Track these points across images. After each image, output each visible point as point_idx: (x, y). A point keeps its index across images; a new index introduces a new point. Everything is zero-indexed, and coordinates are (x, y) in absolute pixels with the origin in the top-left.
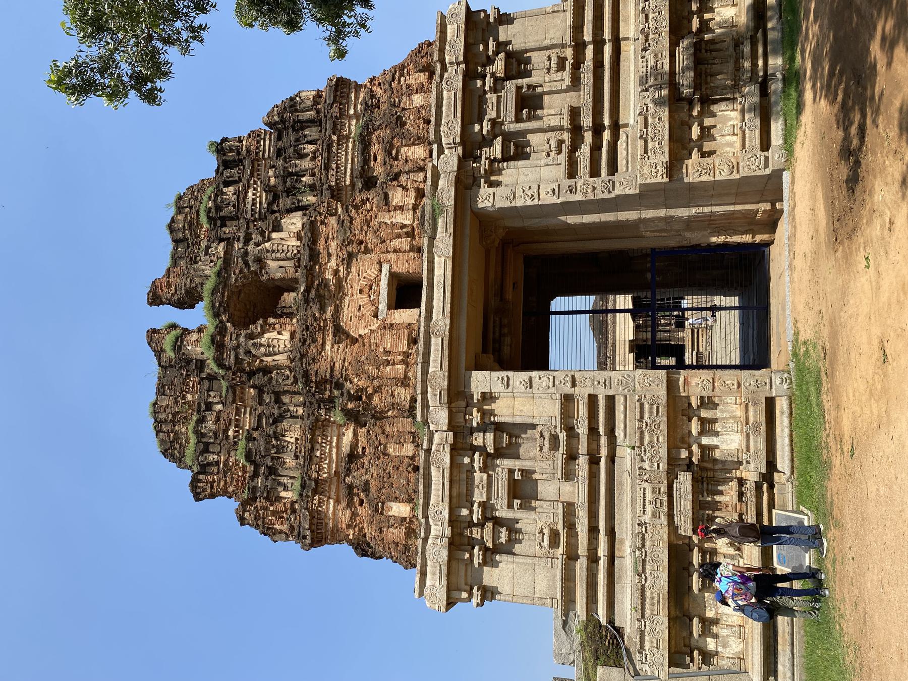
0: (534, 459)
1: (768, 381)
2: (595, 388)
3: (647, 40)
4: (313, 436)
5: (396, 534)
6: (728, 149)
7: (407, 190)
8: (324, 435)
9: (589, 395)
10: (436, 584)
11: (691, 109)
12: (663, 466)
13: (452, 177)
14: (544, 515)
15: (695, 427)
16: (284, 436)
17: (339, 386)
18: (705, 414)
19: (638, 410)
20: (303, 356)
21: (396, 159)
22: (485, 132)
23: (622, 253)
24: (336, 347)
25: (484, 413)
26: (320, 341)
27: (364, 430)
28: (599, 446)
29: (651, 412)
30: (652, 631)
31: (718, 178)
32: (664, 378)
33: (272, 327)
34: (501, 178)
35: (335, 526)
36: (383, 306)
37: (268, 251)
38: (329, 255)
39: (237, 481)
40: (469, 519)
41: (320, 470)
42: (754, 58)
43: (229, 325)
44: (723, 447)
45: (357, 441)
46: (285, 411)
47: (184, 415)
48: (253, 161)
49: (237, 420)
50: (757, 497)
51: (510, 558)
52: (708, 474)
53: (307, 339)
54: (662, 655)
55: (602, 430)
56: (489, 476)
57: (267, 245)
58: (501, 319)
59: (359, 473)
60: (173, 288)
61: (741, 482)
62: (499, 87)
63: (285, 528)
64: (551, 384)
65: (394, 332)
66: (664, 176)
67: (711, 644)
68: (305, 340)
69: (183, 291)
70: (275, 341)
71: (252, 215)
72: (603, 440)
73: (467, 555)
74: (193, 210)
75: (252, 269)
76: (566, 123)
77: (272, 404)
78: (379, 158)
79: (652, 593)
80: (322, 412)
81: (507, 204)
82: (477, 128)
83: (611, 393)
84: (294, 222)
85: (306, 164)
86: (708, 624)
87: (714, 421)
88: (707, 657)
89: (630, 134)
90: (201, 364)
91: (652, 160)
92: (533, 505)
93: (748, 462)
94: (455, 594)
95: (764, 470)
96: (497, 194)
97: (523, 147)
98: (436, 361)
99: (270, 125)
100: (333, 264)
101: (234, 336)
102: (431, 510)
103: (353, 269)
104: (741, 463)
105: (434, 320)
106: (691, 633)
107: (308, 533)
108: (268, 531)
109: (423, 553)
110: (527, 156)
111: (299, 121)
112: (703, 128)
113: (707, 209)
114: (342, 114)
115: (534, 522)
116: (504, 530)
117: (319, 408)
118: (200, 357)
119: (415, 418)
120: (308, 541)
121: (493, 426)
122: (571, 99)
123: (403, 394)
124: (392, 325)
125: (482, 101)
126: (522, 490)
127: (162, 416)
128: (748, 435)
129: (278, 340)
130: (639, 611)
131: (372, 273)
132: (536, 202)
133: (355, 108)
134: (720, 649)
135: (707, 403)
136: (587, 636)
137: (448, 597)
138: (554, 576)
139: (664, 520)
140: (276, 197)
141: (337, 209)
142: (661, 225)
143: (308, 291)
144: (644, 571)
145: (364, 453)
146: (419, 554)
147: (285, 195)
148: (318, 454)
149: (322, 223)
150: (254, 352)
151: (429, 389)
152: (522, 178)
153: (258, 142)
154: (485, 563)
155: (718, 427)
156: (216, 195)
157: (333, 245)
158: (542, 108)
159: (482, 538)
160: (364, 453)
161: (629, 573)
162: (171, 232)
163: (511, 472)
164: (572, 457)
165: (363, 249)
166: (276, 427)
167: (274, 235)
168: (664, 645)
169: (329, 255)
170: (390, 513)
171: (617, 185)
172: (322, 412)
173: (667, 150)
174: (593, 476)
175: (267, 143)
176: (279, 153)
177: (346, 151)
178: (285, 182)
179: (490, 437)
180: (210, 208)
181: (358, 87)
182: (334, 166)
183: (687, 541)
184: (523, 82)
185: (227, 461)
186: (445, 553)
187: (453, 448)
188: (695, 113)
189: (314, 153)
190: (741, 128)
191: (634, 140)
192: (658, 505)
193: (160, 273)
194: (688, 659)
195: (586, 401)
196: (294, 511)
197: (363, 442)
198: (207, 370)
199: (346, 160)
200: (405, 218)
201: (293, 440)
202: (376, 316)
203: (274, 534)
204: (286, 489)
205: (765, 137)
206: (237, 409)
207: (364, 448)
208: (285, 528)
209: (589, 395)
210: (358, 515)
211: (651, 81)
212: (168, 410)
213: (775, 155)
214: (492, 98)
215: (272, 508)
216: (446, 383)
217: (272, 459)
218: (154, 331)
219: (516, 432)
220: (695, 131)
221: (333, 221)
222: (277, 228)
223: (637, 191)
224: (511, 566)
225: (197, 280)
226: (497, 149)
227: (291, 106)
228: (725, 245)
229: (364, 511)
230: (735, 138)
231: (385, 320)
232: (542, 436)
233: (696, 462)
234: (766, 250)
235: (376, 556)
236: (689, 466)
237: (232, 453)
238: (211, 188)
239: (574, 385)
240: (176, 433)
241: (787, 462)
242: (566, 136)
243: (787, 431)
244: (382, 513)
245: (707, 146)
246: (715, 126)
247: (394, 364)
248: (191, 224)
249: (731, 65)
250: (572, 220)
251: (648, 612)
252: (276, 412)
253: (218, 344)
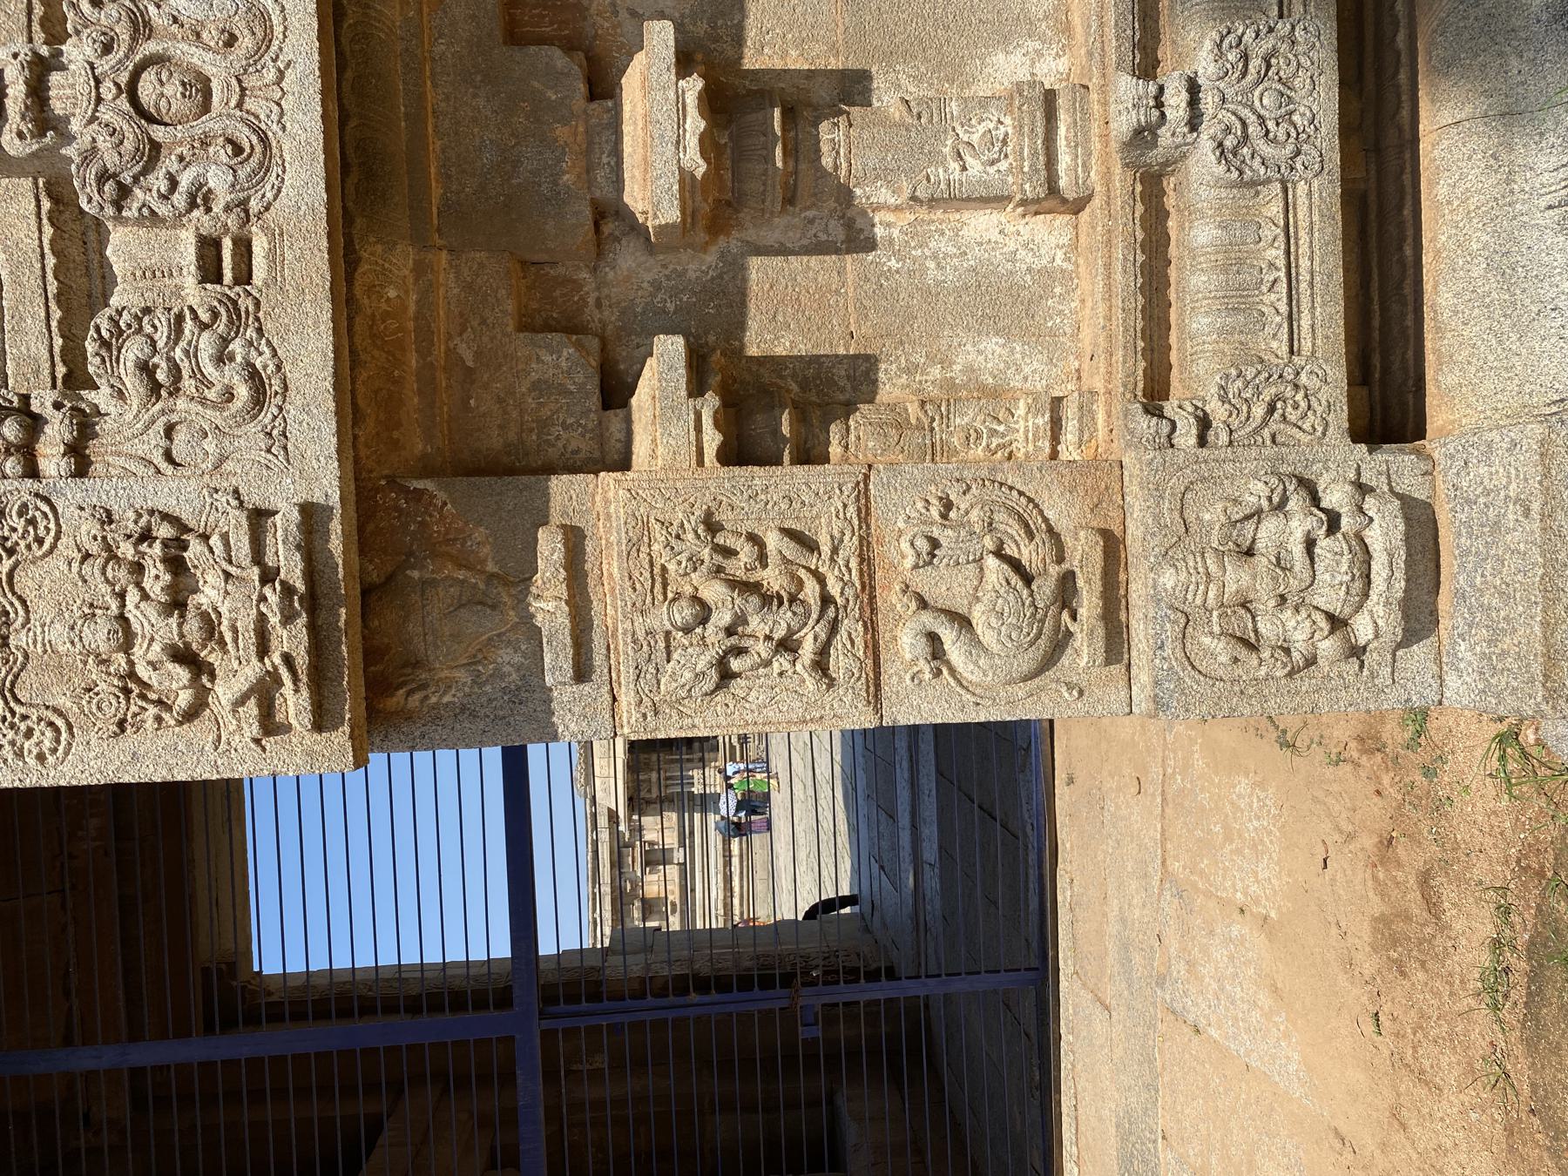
6: (985, 354)
66: (294, 703)
91: (129, 481)
173: (306, 348)
190: (1143, 136)
220: (657, 134)
230: (1048, 236)
246: (851, 88)
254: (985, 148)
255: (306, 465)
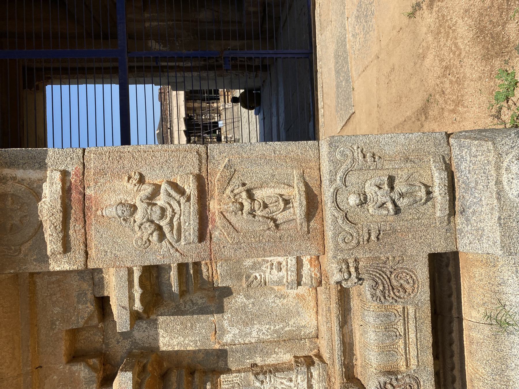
18: (173, 336)
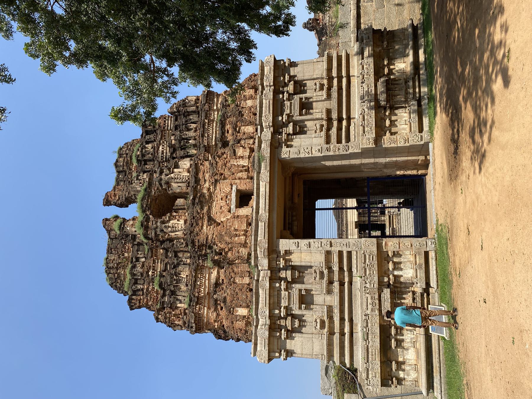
0: (312, 283)
1: (425, 243)
2: (342, 247)
3: (363, 78)
4: (196, 274)
5: (240, 324)
6: (403, 131)
7: (245, 148)
8: (202, 274)
9: (339, 251)
10: (262, 349)
11: (385, 112)
12: (376, 286)
13: (269, 143)
14: (317, 312)
15: (391, 266)
16: (180, 274)
17: (210, 248)
18: (395, 260)
19: (363, 258)
20: (191, 232)
21: (239, 132)
22: (284, 121)
23: (352, 179)
24: (209, 227)
25: (286, 261)
26: (201, 224)
27: (223, 270)
28: (344, 277)
29: (369, 259)
30: (373, 368)
31: (399, 145)
32: (376, 242)
33: (175, 217)
34: (292, 143)
35: (208, 321)
36: (233, 206)
37: (172, 178)
38: (205, 181)
39: (154, 299)
40: (279, 315)
41: (199, 292)
42: (414, 88)
43: (151, 216)
44: (405, 276)
45: (219, 276)
46: (180, 261)
47: (123, 264)
48: (162, 131)
49: (153, 266)
50: (421, 300)
51: (300, 335)
52: (398, 289)
53: (193, 223)
54: (378, 380)
55: (345, 269)
56: (289, 293)
57: (172, 175)
58: (292, 213)
59: (221, 293)
60: (117, 197)
61: (414, 293)
62: (291, 98)
63: (181, 323)
64: (320, 246)
65: (239, 220)
67: (401, 374)
68: (192, 224)
69: (124, 199)
70: (176, 225)
71: (162, 159)
72: (346, 274)
73: (278, 334)
74: (128, 156)
75: (164, 187)
76: (324, 116)
77: (173, 257)
78: (230, 132)
79: (372, 350)
80: (200, 261)
81: (296, 156)
82: (280, 118)
83: (350, 250)
84: (186, 164)
85: (191, 134)
86: (400, 364)
87: (400, 263)
88: (400, 381)
89: (356, 123)
90: (134, 237)
91: (367, 136)
92: (312, 307)
93: (417, 283)
94: (272, 354)
95: (424, 287)
96: (291, 151)
97: (303, 128)
98: (261, 234)
99: (172, 113)
100: (207, 185)
101: (154, 222)
102: (260, 311)
103: (218, 188)
104: (413, 284)
105: (260, 213)
106: (392, 369)
107: (194, 325)
108: (172, 325)
109: (256, 333)
110: (305, 133)
111: (188, 112)
112: (391, 121)
113: (394, 159)
114: (210, 109)
115: (312, 316)
116: (297, 321)
117: (199, 259)
118: (134, 233)
119: (250, 264)
120: (194, 329)
121: (290, 267)
122: (327, 105)
123: (244, 252)
124: (238, 216)
125: (282, 105)
126: (306, 300)
127: (111, 265)
128: (416, 270)
129: (178, 225)
130: (366, 359)
131: (228, 189)
132: (310, 155)
133: (217, 106)
134: (406, 377)
135: (397, 254)
136: (339, 379)
137: (269, 356)
138: (323, 343)
139: (377, 312)
140: (175, 150)
141: (208, 157)
142: (372, 166)
143: (194, 199)
144: (368, 338)
145: (223, 283)
146: (253, 334)
147: (179, 150)
148: (199, 283)
149: (201, 164)
150: (165, 230)
151: (258, 249)
152: (303, 143)
153: (165, 121)
154: (287, 338)
155: (402, 266)
156: (142, 149)
157: (207, 176)
158: (312, 109)
159: (286, 325)
160: (223, 283)
161: (360, 340)
162: (116, 167)
163: (300, 290)
164: (331, 282)
165: (223, 177)
166: (176, 270)
167: (175, 170)
168: (378, 375)
169: (205, 181)
170: (237, 314)
171: (350, 148)
172: (200, 261)
173: (374, 132)
174: (342, 292)
175: (170, 122)
176: (176, 127)
177: (212, 127)
178: (180, 143)
179: (289, 273)
180: (138, 155)
181: (218, 95)
182: (206, 135)
183: (388, 323)
184: (303, 96)
185: (148, 289)
186: (267, 333)
187: (271, 279)
188: (387, 114)
189: (196, 128)
191: (358, 126)
192: (374, 305)
193: (110, 189)
194: (390, 382)
195: (337, 254)
196: (185, 314)
197: (222, 276)
198: (137, 240)
199: (213, 132)
200: (245, 162)
201: (185, 276)
202: (229, 211)
203: (174, 326)
204: (181, 302)
205: (420, 126)
206: (154, 261)
207: (223, 280)
208: (181, 323)
209: (339, 251)
210: (220, 315)
211: (366, 98)
212: (114, 262)
213: (425, 135)
214: (287, 103)
215: (173, 313)
216: (267, 245)
217: (174, 286)
218: (107, 220)
219: (302, 270)
220: (388, 123)
221: (207, 163)
222: (177, 166)
223: (360, 151)
224: (301, 339)
225: (132, 193)
226: (290, 129)
227: (183, 104)
228: (404, 176)
229: (223, 313)
230: (406, 126)
231: (234, 213)
232: (315, 272)
233: (392, 283)
234: (424, 178)
235: (226, 338)
236: (389, 286)
237: (151, 284)
238: (139, 145)
239: (331, 246)
240: (118, 274)
241: (435, 282)
242: (324, 123)
243: (434, 267)
244: (233, 314)
245: (394, 130)
246: (397, 120)
247: (239, 236)
248: (127, 163)
249: (403, 92)
250: (328, 163)
251: (370, 359)
252: (176, 262)
253: (145, 226)
254: (403, 122)
255: (374, 135)
